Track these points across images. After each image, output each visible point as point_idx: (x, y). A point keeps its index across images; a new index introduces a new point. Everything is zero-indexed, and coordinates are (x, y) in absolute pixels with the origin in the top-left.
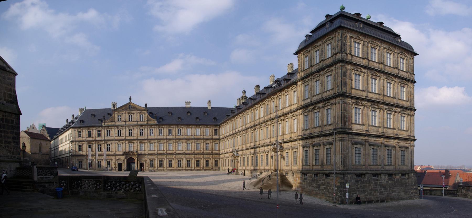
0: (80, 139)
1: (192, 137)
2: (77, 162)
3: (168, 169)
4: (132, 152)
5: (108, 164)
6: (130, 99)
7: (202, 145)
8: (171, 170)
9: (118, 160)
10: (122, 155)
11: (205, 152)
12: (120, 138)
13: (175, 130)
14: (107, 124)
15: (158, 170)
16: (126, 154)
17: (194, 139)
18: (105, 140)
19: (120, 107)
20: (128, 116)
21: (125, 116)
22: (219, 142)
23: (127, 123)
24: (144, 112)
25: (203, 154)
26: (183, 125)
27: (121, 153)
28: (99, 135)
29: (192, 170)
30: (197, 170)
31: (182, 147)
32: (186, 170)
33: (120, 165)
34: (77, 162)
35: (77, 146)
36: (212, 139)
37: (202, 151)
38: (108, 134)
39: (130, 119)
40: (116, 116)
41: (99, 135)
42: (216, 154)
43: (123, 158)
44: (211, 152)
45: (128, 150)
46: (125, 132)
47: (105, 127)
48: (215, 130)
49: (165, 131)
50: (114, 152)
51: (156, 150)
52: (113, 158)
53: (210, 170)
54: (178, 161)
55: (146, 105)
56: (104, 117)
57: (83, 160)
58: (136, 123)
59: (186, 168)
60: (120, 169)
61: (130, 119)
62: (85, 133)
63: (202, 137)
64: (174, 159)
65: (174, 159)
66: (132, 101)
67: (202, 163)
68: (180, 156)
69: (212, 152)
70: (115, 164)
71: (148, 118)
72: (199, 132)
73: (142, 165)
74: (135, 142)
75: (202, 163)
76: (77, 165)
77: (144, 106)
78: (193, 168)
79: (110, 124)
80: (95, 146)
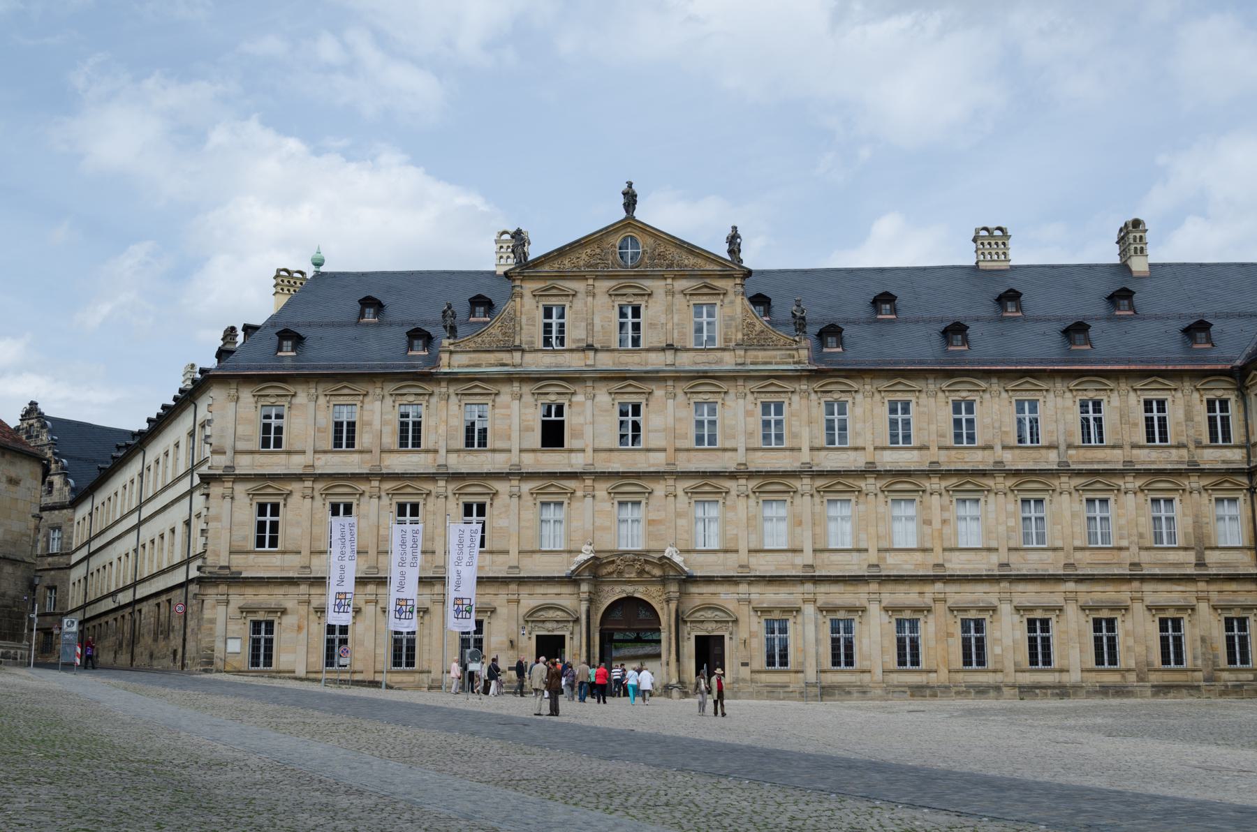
2: (243, 629)
3: (896, 678)
6: (630, 200)
8: (918, 691)
12: (553, 460)
15: (826, 692)
19: (561, 252)
21: (592, 311)
23: (605, 362)
24: (719, 283)
26: (987, 375)
29: (1063, 691)
30: (1105, 690)
34: (234, 627)
35: (246, 515)
40: (527, 309)
44: (1191, 557)
46: (592, 420)
47: (453, 379)
48: (1211, 405)
49: (867, 411)
50: (513, 558)
51: (808, 548)
53: (1193, 688)
54: (965, 625)
55: (734, 240)
57: (284, 612)
58: (669, 356)
59: (1027, 678)
62: (308, 416)
66: (639, 214)
67: (1138, 636)
73: (709, 653)
74: (659, 488)
75: (1138, 636)
76: (234, 646)
77: (722, 251)
78: (1074, 677)
79: (488, 363)
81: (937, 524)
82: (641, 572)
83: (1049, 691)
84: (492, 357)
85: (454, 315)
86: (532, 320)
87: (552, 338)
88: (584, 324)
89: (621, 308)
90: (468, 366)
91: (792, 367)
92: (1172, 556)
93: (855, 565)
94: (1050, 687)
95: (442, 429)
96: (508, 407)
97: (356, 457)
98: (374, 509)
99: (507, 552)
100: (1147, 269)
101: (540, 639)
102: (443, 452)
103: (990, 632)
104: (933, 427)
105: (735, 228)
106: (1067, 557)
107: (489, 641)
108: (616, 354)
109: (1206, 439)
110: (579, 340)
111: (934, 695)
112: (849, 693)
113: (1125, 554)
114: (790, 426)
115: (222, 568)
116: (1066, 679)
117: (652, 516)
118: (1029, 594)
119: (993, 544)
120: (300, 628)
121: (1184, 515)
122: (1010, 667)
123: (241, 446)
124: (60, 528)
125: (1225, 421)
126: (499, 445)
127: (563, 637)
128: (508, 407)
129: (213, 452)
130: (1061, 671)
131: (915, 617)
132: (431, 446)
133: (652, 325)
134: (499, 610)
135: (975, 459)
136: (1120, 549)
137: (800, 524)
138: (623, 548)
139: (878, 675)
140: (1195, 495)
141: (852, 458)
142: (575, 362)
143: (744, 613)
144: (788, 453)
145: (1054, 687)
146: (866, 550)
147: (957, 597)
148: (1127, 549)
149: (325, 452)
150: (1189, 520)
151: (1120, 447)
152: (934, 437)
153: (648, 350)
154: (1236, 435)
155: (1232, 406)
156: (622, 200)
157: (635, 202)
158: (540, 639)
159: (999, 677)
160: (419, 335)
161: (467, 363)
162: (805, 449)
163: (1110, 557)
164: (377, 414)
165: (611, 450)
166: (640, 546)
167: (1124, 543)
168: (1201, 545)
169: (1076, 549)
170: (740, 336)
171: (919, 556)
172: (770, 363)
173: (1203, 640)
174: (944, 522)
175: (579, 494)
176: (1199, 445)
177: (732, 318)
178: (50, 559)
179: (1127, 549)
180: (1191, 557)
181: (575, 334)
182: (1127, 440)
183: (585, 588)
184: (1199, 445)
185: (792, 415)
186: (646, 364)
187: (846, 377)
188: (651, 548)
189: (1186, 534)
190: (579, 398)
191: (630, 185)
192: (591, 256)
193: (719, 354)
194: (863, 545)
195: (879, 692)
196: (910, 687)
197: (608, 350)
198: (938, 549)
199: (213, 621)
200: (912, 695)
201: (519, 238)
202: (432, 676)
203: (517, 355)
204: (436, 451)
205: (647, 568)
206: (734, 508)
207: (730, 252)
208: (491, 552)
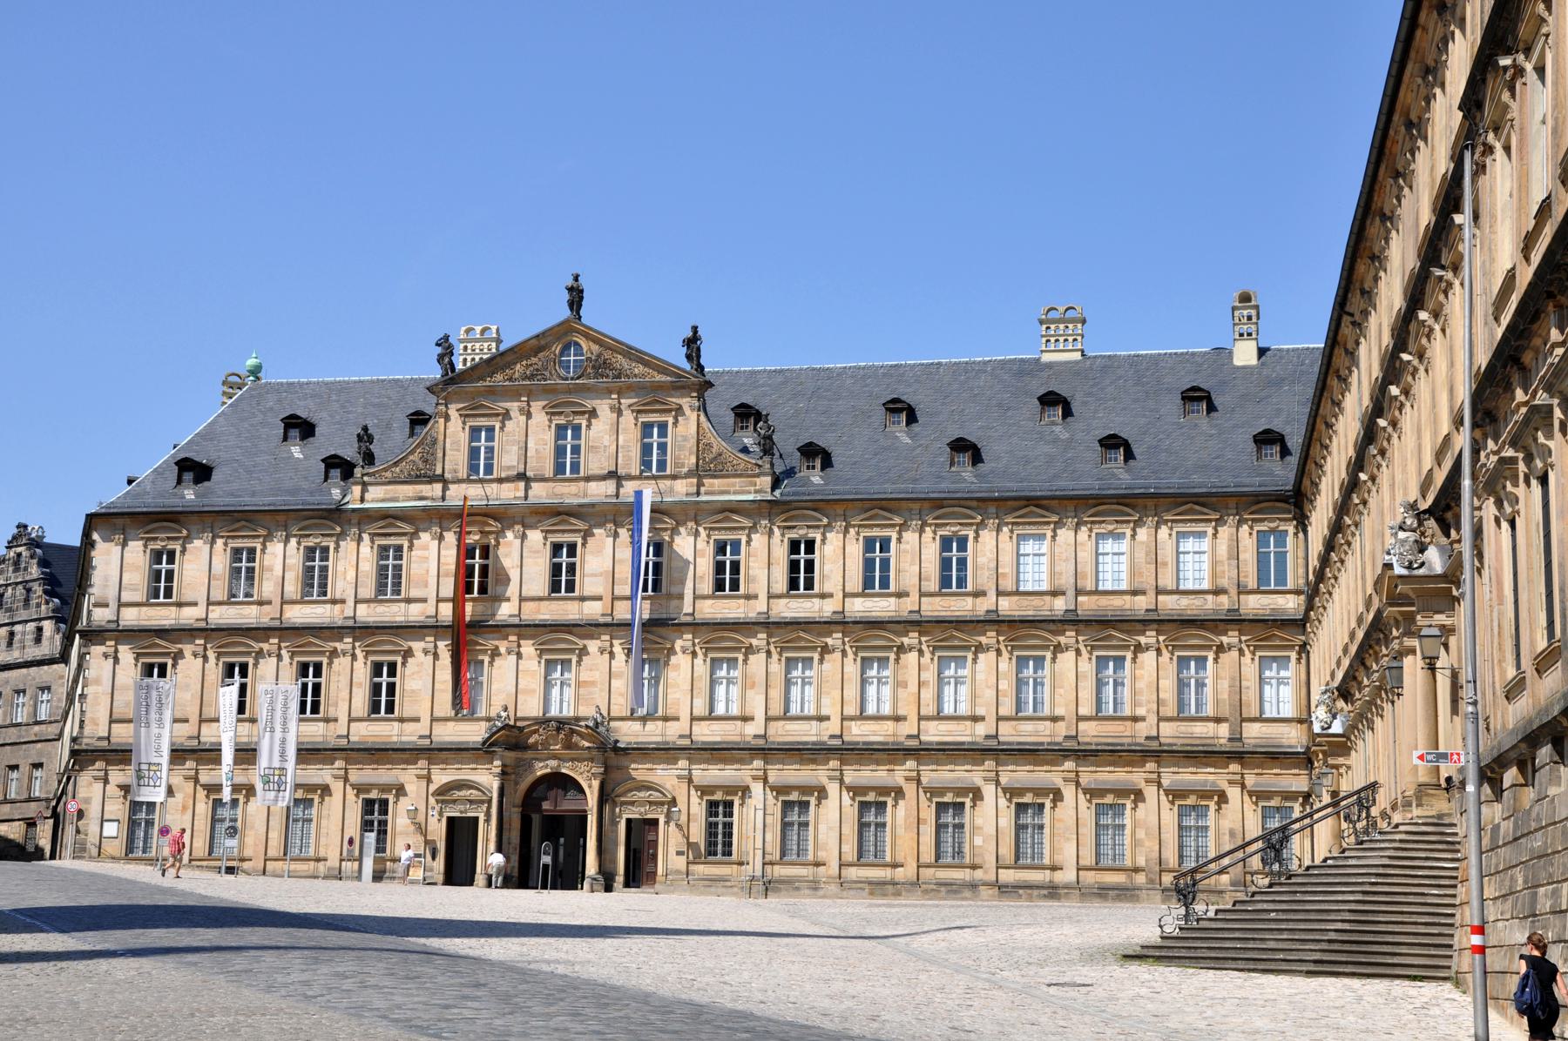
0: (163, 616)
1: (1060, 605)
2: (117, 808)
3: (853, 873)
4: (561, 723)
5: (367, 826)
6: (576, 297)
7: (1149, 675)
8: (878, 888)
9: (444, 790)
10: (483, 752)
11: (1168, 731)
13: (915, 553)
14: (377, 497)
16: (510, 740)
17: (1073, 621)
18: (361, 631)
20: (550, 436)
21: (527, 434)
22: (1304, 649)
23: (541, 493)
25: (1154, 753)
27: (474, 733)
28: (315, 582)
29: (1053, 892)
31: (979, 689)
32: (1004, 890)
33: (461, 835)
36: (1234, 621)
37: (1143, 730)
38: (389, 581)
39: (565, 464)
40: (453, 432)
41: (315, 582)
42: (1275, 757)
43: (487, 778)
44: (1224, 730)
45: (531, 707)
50: (422, 728)
52: (408, 776)
55: (692, 343)
56: (365, 437)
58: (609, 487)
59: (1008, 876)
60: (459, 870)
61: (565, 464)
62: (201, 564)
63: (1142, 603)
64: (899, 793)
65: (899, 793)
69: (1236, 738)
70: (421, 829)
71: (701, 447)
72: (1114, 561)
78: (1068, 876)
79: (405, 497)
80: (275, 680)
81: (913, 687)
82: (569, 745)
83: (1036, 892)
84: (409, 490)
85: (370, 439)
86: (456, 443)
87: (479, 466)
88: (515, 448)
89: (558, 427)
90: (383, 500)
91: (751, 497)
92: (1201, 730)
93: (808, 733)
94: (1038, 887)
95: (351, 574)
96: (426, 548)
97: (253, 610)
98: (193, 670)
99: (417, 720)
100: (1254, 361)
101: (451, 820)
102: (351, 602)
105: (695, 329)
106: (1067, 728)
107: (394, 822)
108: (551, 484)
109: (1252, 583)
110: (509, 468)
111: (898, 894)
112: (797, 889)
113: (1140, 725)
114: (748, 568)
115: (100, 739)
117: (584, 676)
118: (1018, 774)
119: (980, 711)
120: (184, 808)
121: (1217, 677)
123: (126, 597)
124: (49, 688)
125: (1281, 558)
126: (414, 593)
127: (477, 819)
128: (426, 548)
129: (96, 605)
130: (974, 867)
131: (882, 799)
132: (338, 596)
133: (591, 449)
134: (408, 788)
135: (961, 607)
136: (1135, 719)
137: (753, 687)
138: (554, 712)
139: (833, 868)
141: (816, 608)
142: (509, 493)
143: (681, 792)
144: (742, 601)
145: (1042, 887)
146: (828, 718)
147: (934, 774)
148: (1143, 719)
149: (220, 603)
150: (1224, 685)
151: (1143, 593)
153: (588, 479)
155: (1290, 539)
156: (566, 296)
157: (581, 298)
158: (451, 820)
159: (979, 874)
160: (339, 466)
161: (381, 496)
162: (763, 596)
163: (1121, 728)
164: (280, 559)
165: (540, 599)
166: (568, 712)
167: (1140, 712)
169: (1080, 719)
170: (693, 460)
171: (889, 726)
172: (728, 492)
175: (503, 650)
176: (1242, 590)
177: (685, 439)
178: (37, 728)
179: (1143, 719)
180: (1224, 730)
181: (508, 459)
182: (1148, 581)
183: (497, 763)
184: (1242, 590)
185: (749, 555)
186: (585, 495)
187: (815, 510)
188: (581, 714)
189: (1217, 702)
190: (510, 535)
191: (576, 278)
192: (528, 366)
193: (668, 482)
194: (824, 712)
195: (833, 888)
196: (870, 883)
197: (543, 480)
198: (913, 718)
199: (87, 801)
200: (871, 893)
201: (446, 349)
202: (328, 864)
203: (438, 487)
204: (343, 602)
205: (575, 738)
206: (677, 667)
207: (689, 357)
208: (401, 720)
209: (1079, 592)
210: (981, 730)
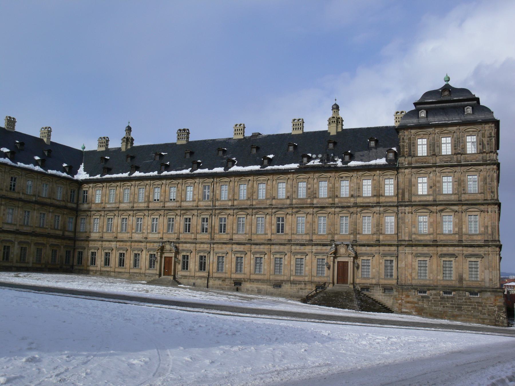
1: (34, 199)
17: (36, 202)
22: (77, 217)
25: (49, 236)
42: (69, 238)
59: (18, 265)
68: (10, 237)
69: (63, 235)
78: (30, 265)
103: (11, 250)
104: (5, 184)
109: (69, 200)
116: (28, 265)
122: (15, 261)
125: (74, 196)
135: (15, 195)
136: (46, 228)
140: (65, 216)
152: (5, 187)
154: (75, 201)
155: (76, 192)
167: (47, 227)
168: (64, 229)
173: (61, 256)
174: (4, 214)
184: (67, 201)
209: (39, 196)
210: (15, 228)
